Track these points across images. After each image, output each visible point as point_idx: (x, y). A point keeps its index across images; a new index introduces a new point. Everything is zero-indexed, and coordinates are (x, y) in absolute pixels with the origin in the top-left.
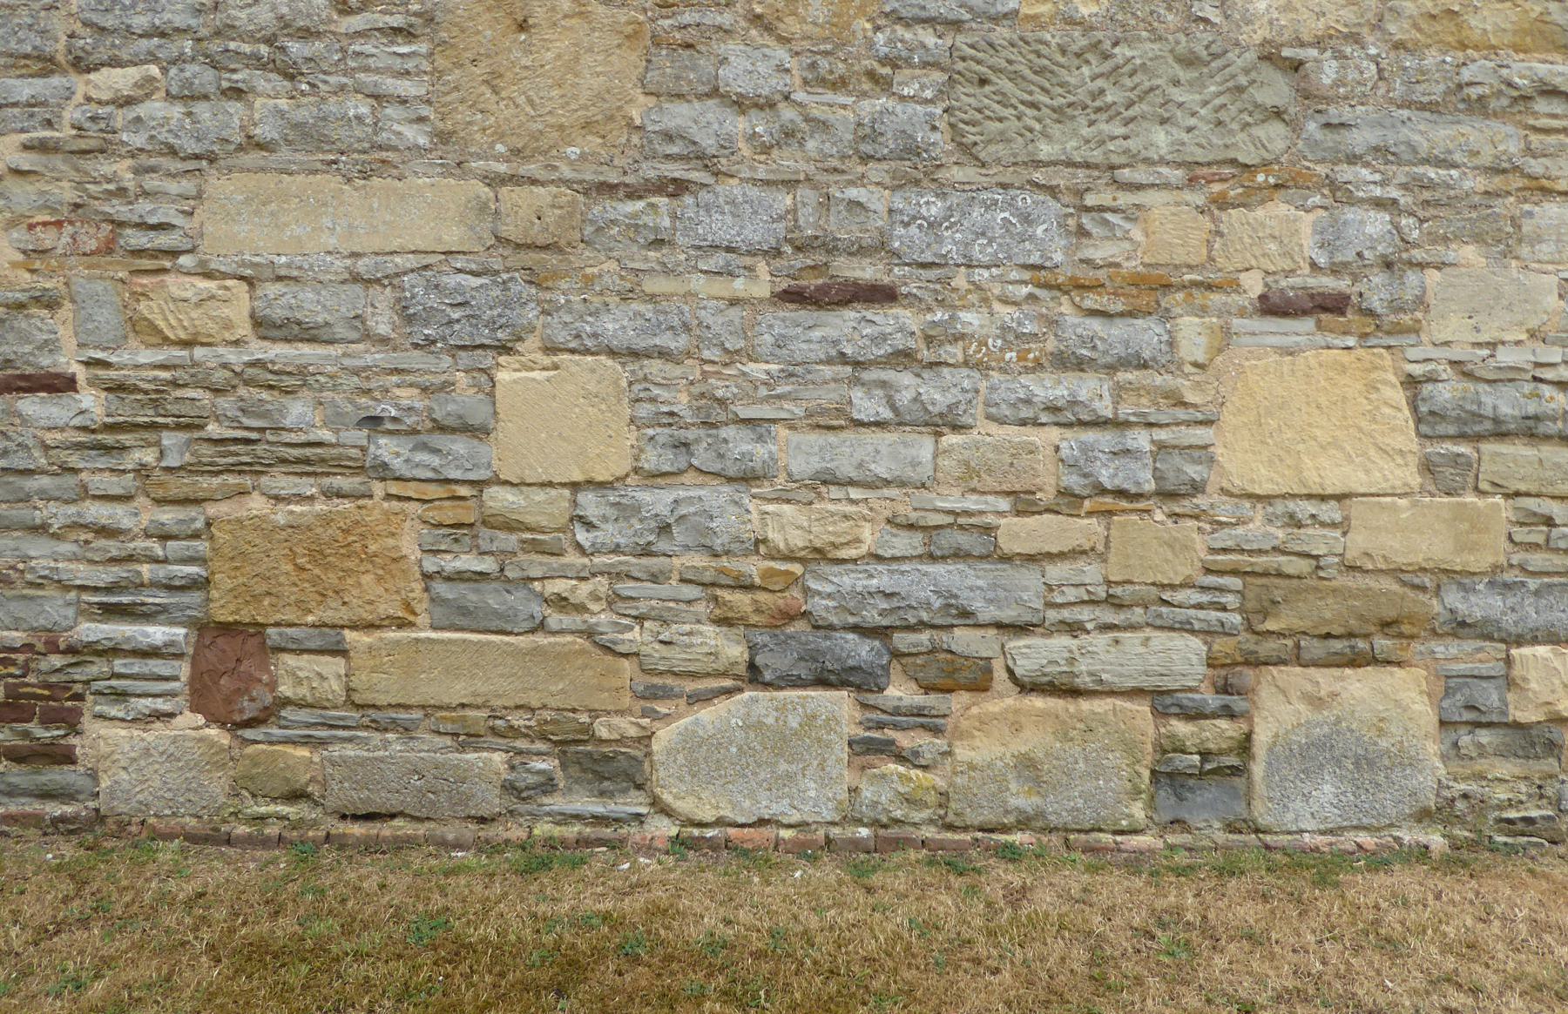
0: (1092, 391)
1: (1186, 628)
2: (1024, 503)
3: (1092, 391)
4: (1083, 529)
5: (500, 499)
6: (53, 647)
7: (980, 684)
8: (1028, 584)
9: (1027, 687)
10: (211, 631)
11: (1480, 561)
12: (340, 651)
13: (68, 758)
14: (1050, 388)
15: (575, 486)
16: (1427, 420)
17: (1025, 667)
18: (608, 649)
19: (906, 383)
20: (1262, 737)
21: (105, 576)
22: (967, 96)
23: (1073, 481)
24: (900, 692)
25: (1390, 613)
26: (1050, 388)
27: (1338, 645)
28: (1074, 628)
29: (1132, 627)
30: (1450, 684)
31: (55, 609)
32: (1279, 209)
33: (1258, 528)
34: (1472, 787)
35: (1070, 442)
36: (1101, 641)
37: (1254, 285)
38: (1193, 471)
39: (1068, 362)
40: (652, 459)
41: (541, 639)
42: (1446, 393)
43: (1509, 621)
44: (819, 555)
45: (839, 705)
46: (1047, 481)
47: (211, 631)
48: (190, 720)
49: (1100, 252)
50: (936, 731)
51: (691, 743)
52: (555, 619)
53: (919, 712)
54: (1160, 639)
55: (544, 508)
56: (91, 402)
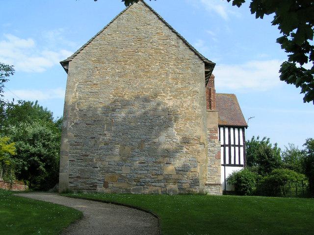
0: (156, 168)
3: (156, 168)
4: (156, 176)
5: (122, 174)
8: (153, 180)
10: (104, 182)
14: (154, 168)
19: (146, 168)
22: (149, 152)
24: (145, 186)
26: (154, 168)
31: (96, 181)
32: (167, 158)
33: (167, 177)
35: (155, 171)
37: (165, 162)
39: (155, 167)
46: (154, 173)
47: (104, 182)
48: (103, 187)
49: (157, 160)
51: (133, 189)
55: (124, 175)
56: (99, 169)
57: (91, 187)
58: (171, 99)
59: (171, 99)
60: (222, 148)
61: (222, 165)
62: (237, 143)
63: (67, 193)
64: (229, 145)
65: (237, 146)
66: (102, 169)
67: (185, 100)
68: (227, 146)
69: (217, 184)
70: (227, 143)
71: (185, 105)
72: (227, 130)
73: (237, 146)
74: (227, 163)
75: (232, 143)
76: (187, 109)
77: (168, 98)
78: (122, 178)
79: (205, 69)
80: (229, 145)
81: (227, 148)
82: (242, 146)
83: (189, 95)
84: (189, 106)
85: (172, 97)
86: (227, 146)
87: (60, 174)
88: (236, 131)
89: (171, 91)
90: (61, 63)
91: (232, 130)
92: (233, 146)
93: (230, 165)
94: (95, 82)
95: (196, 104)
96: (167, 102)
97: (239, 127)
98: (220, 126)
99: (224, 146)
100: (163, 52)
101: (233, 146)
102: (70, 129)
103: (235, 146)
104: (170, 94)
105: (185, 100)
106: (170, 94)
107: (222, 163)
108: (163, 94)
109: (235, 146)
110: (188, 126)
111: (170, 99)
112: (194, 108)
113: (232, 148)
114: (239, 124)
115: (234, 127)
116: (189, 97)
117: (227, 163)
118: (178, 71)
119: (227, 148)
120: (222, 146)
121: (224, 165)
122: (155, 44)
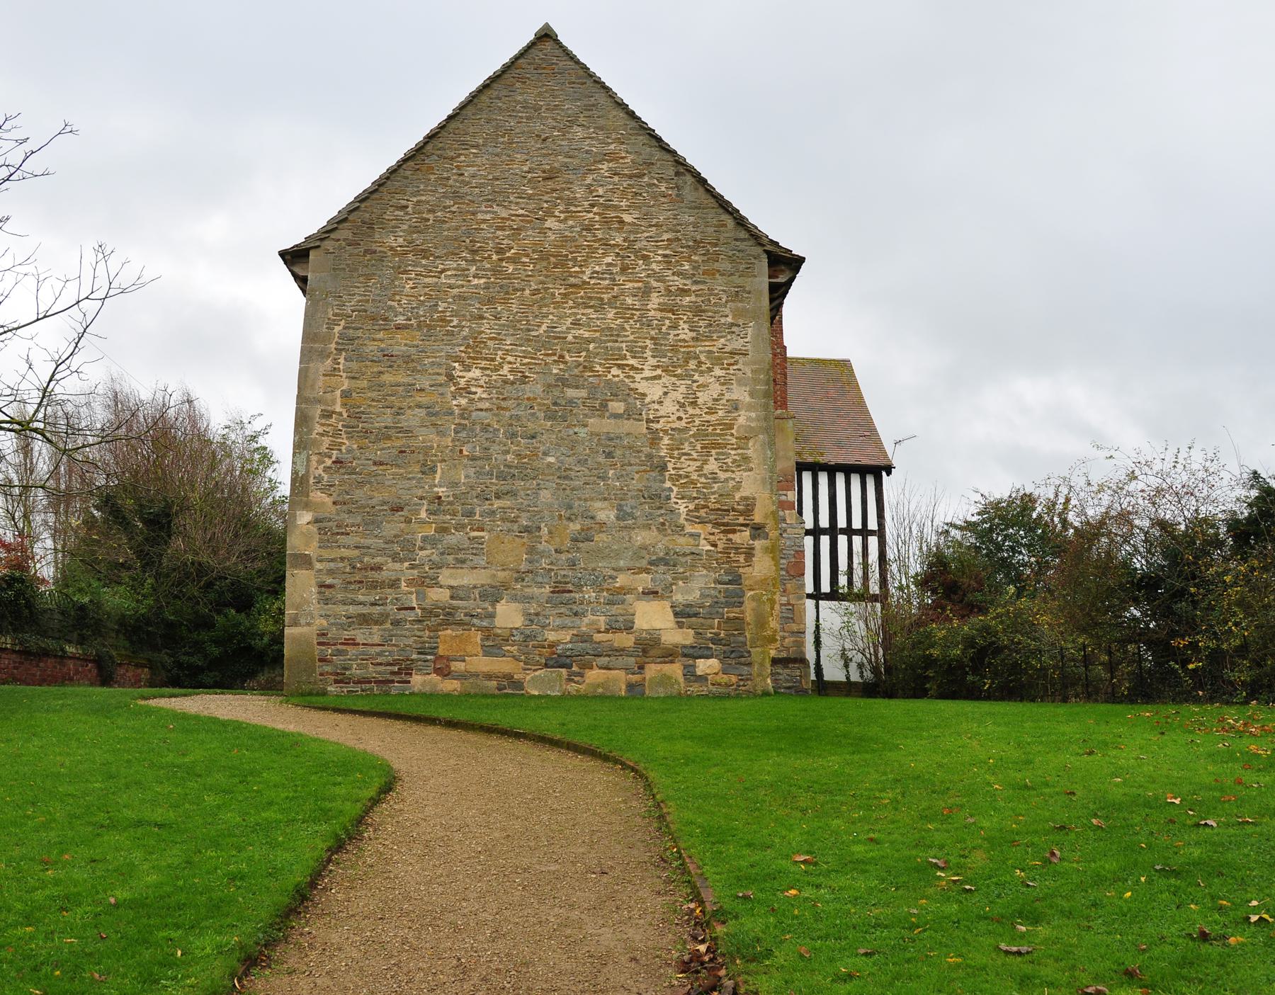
1: (631, 656)
2: (599, 632)
6: (408, 660)
7: (591, 668)
9: (601, 668)
11: (688, 642)
12: (464, 661)
13: (409, 682)
15: (512, 628)
16: (676, 614)
17: (599, 664)
18: (517, 660)
20: (647, 678)
21: (419, 646)
23: (608, 627)
24: (575, 668)
25: (671, 653)
27: (662, 659)
28: (609, 656)
29: (621, 655)
30: (685, 667)
34: (691, 689)
36: (613, 658)
37: (640, 589)
38: (631, 625)
40: (527, 623)
41: (504, 659)
42: (677, 609)
43: (695, 654)
44: (558, 643)
45: (564, 671)
50: (582, 677)
52: (507, 654)
53: (579, 673)
54: (625, 658)
57: (393, 673)
58: (659, 377)
59: (659, 377)
60: (809, 541)
61: (809, 596)
62: (857, 524)
63: (312, 699)
64: (833, 531)
65: (857, 532)
66: (429, 613)
67: (701, 380)
68: (824, 532)
69: (795, 660)
70: (824, 522)
71: (703, 397)
72: (823, 479)
73: (857, 532)
74: (826, 587)
75: (842, 523)
76: (711, 411)
77: (647, 373)
78: (494, 643)
79: (770, 277)
80: (833, 531)
81: (825, 540)
82: (872, 533)
83: (717, 361)
84: (715, 400)
85: (659, 372)
86: (824, 532)
87: (287, 631)
88: (855, 481)
89: (653, 350)
90: (283, 254)
91: (840, 479)
92: (843, 531)
93: (834, 595)
94: (400, 320)
95: (740, 394)
96: (642, 387)
97: (863, 471)
98: (801, 467)
99: (816, 532)
100: (627, 218)
101: (843, 531)
102: (319, 480)
103: (849, 531)
104: (653, 361)
105: (701, 380)
106: (653, 361)
107: (809, 588)
108: (632, 362)
109: (849, 531)
110: (712, 466)
111: (655, 378)
112: (735, 406)
113: (842, 540)
114: (865, 461)
115: (848, 470)
116: (718, 372)
117: (826, 587)
118: (679, 282)
119: (825, 540)
120: (808, 532)
121: (817, 596)
122: (601, 191)
